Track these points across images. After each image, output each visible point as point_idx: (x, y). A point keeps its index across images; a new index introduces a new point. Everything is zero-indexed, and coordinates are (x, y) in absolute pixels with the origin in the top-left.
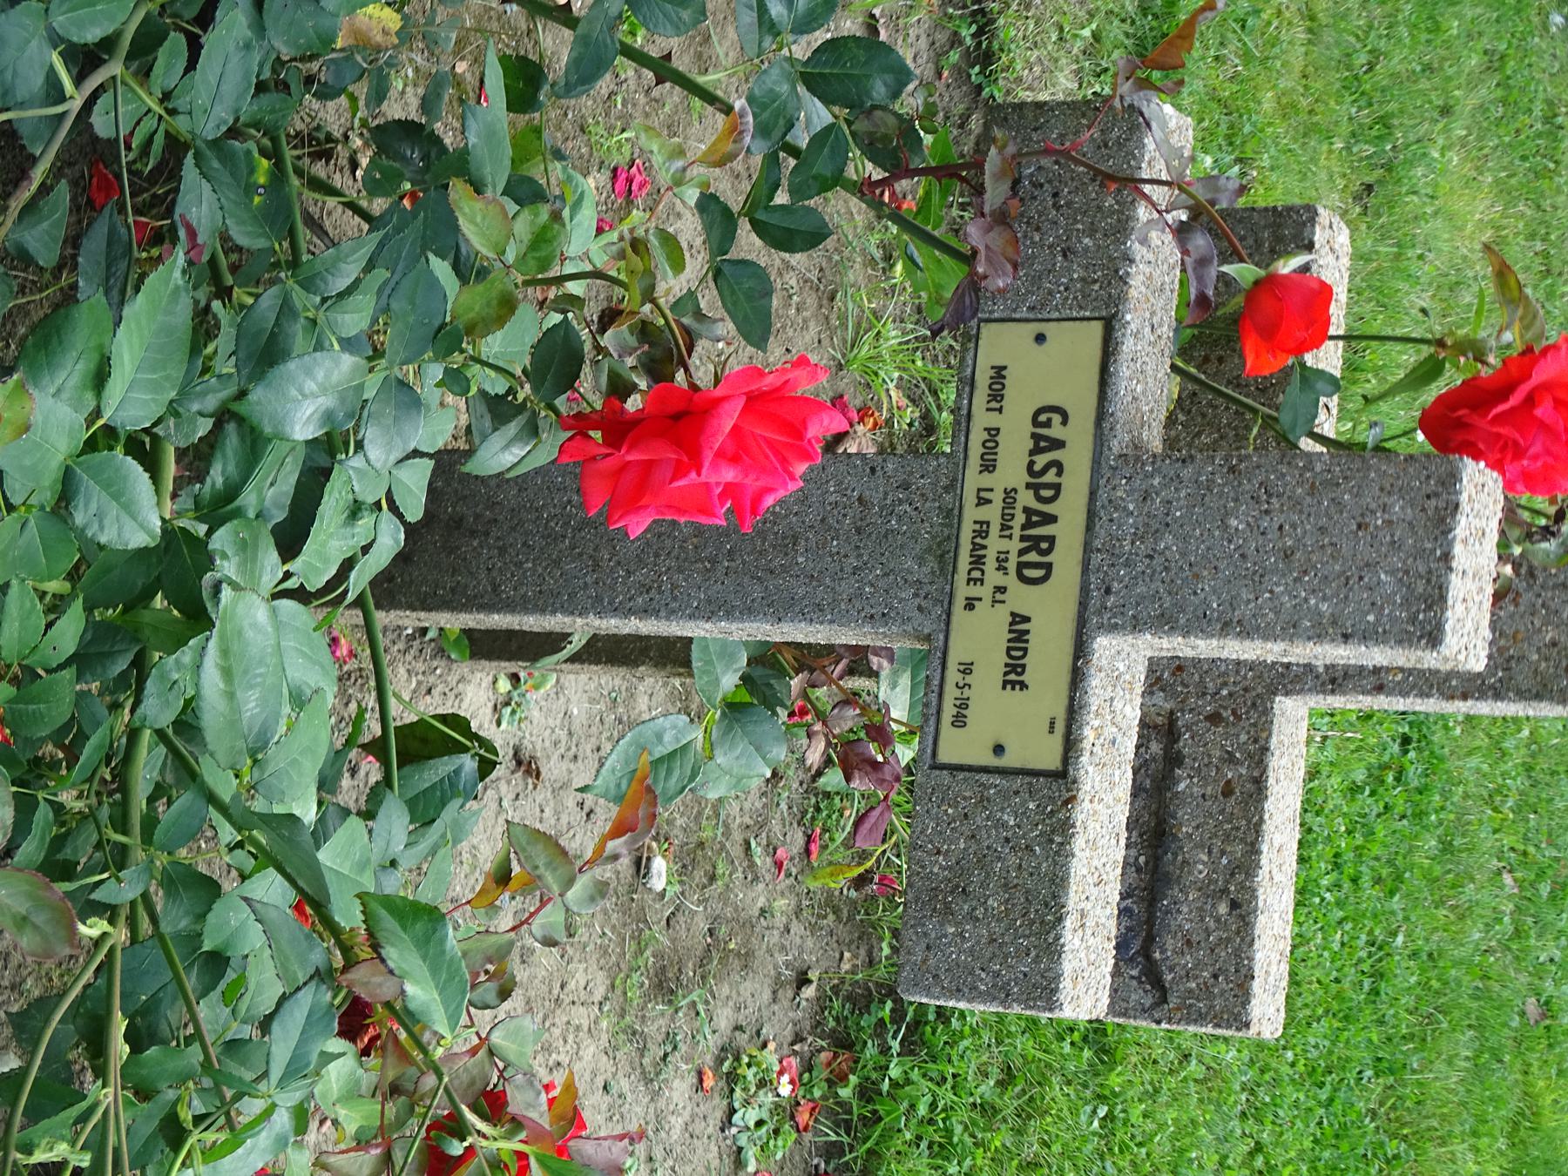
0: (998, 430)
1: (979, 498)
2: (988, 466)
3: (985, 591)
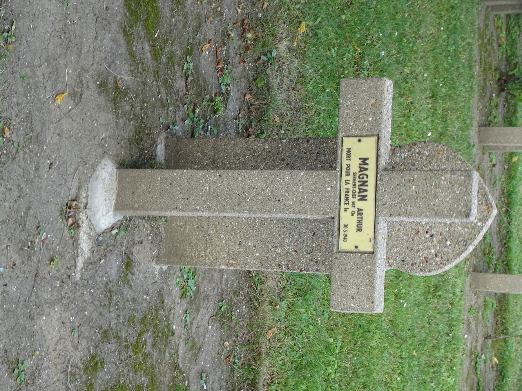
2: (348, 174)
3: (350, 206)
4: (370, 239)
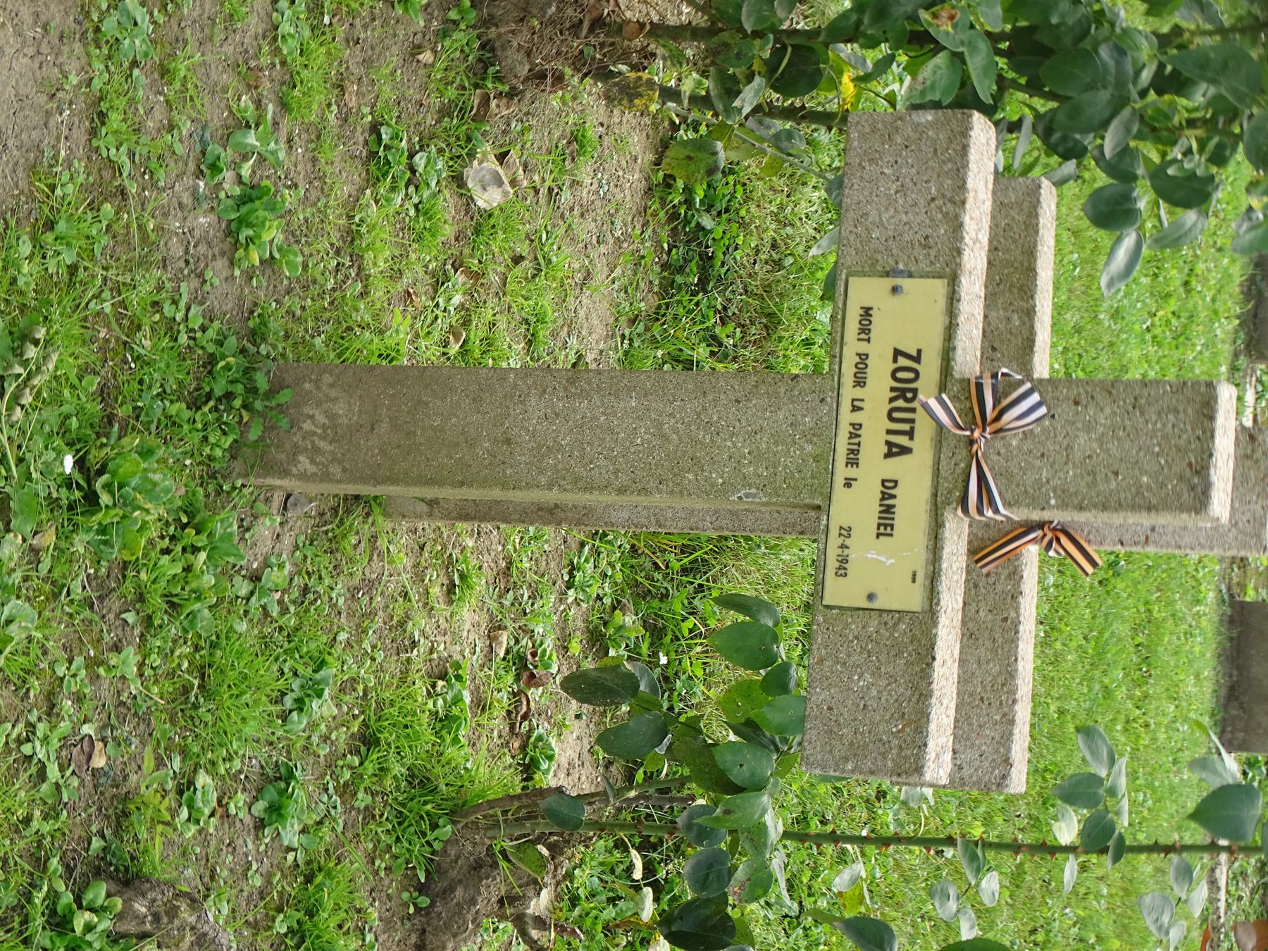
0: (867, 355)
1: (853, 406)
2: (860, 382)
4: (914, 575)
